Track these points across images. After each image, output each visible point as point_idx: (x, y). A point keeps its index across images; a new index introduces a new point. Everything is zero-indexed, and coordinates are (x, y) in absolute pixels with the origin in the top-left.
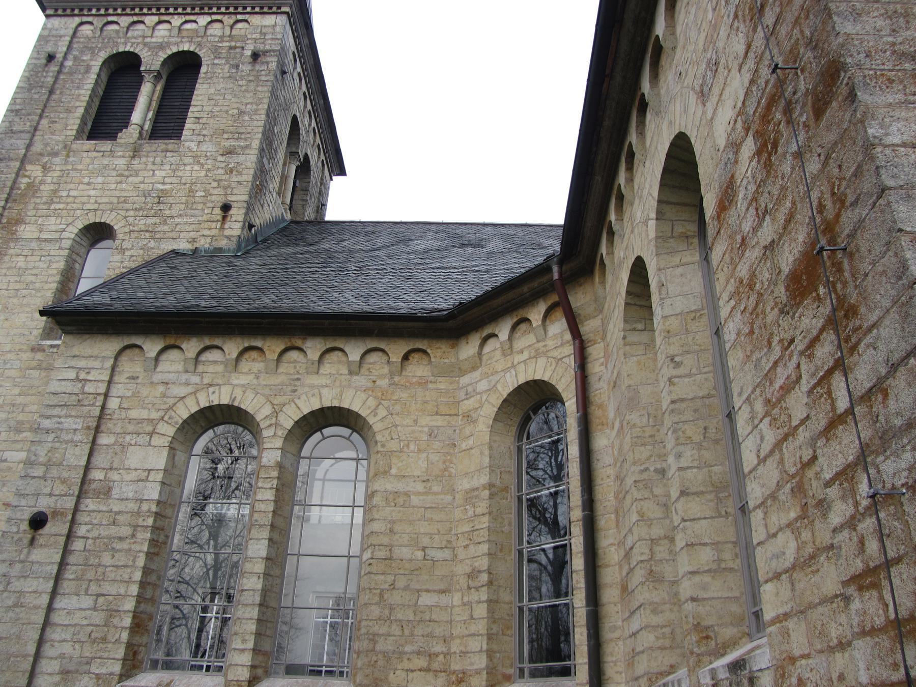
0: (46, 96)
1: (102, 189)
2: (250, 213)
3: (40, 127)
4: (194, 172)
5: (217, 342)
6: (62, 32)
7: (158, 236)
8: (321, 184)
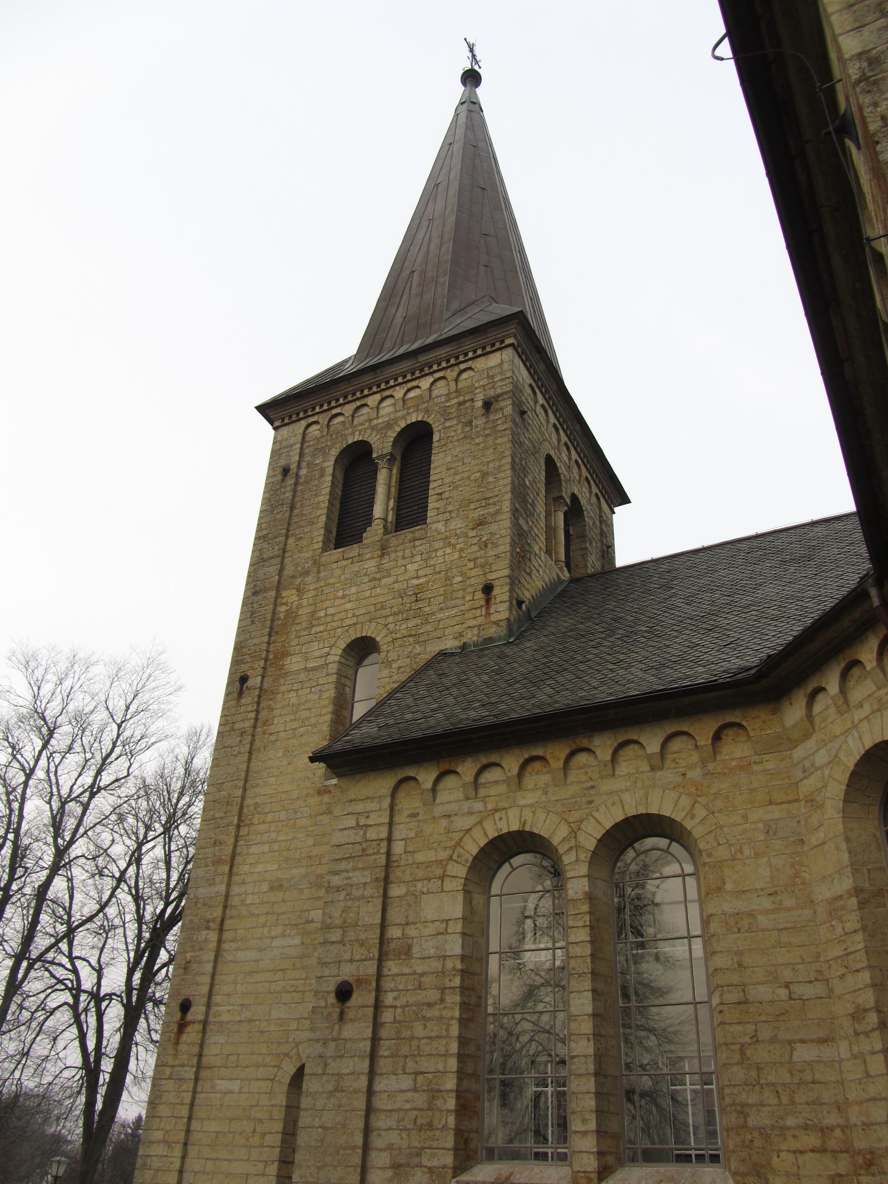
0: (288, 513)
3: (288, 548)
4: (447, 556)
5: (494, 758)
6: (292, 441)
7: (422, 639)
8: (601, 523)
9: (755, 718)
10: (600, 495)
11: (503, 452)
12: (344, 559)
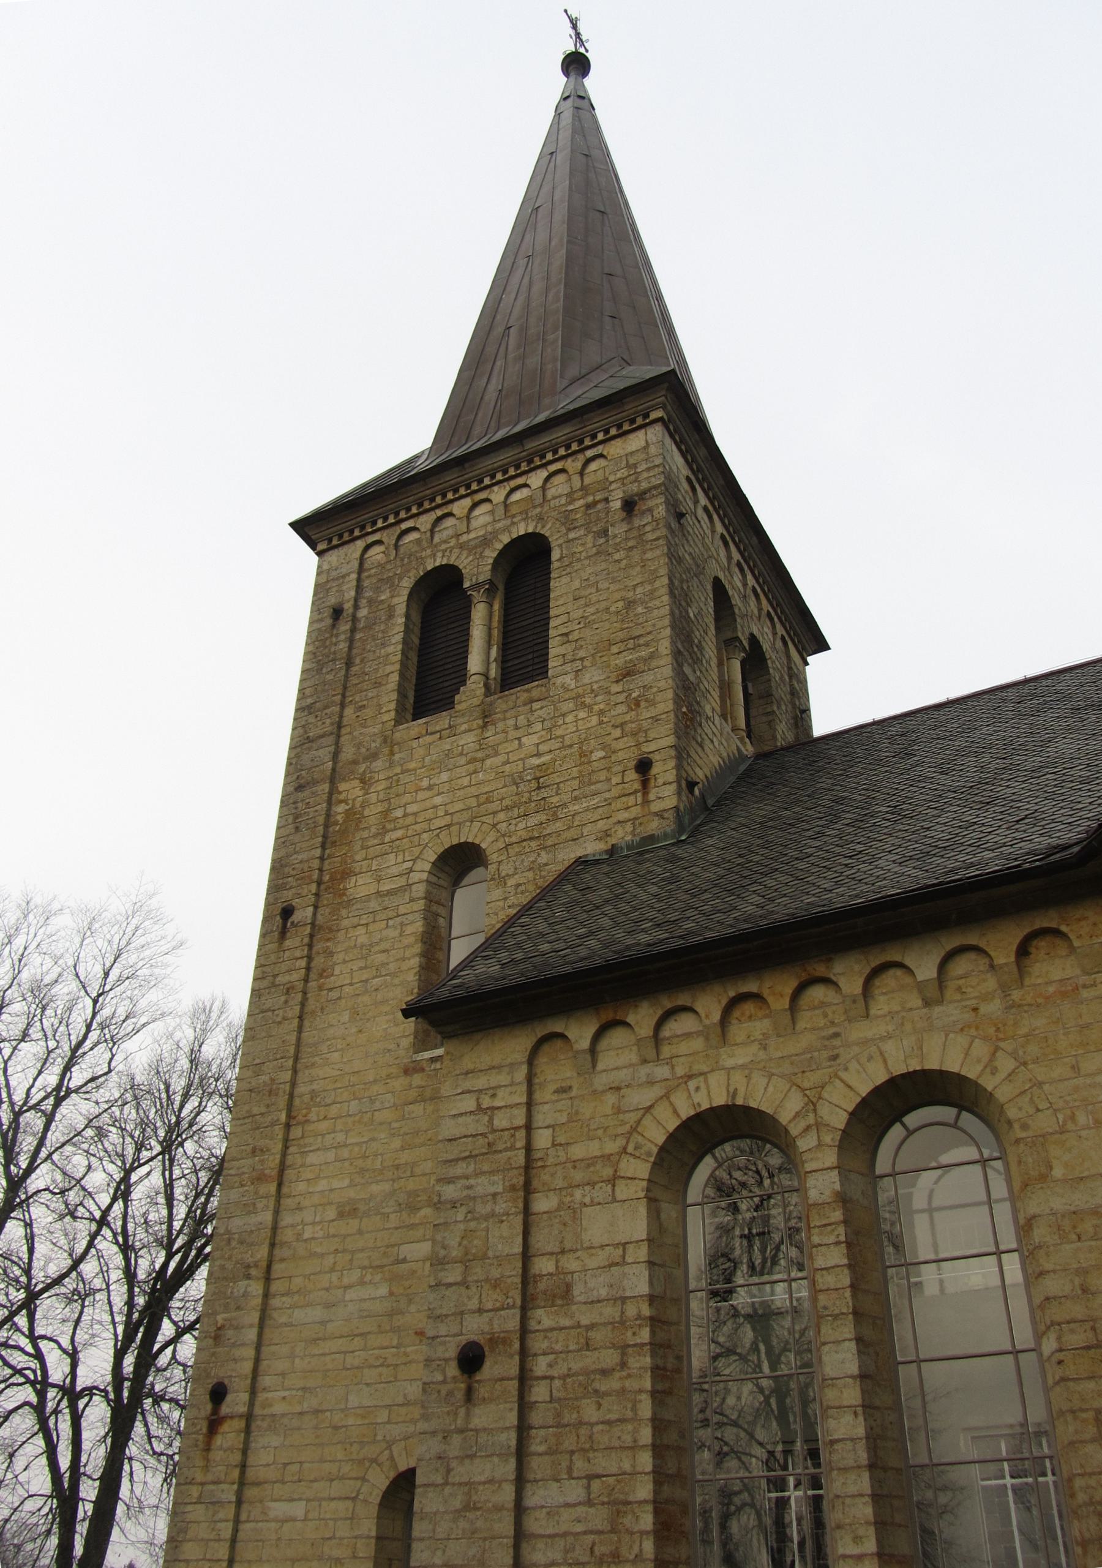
0: (343, 672)
1: (452, 790)
2: (685, 763)
3: (345, 721)
4: (580, 722)
5: (683, 999)
6: (344, 571)
7: (549, 843)
8: (790, 677)
9: (1079, 920)
10: (787, 638)
11: (656, 570)
12: (427, 733)
